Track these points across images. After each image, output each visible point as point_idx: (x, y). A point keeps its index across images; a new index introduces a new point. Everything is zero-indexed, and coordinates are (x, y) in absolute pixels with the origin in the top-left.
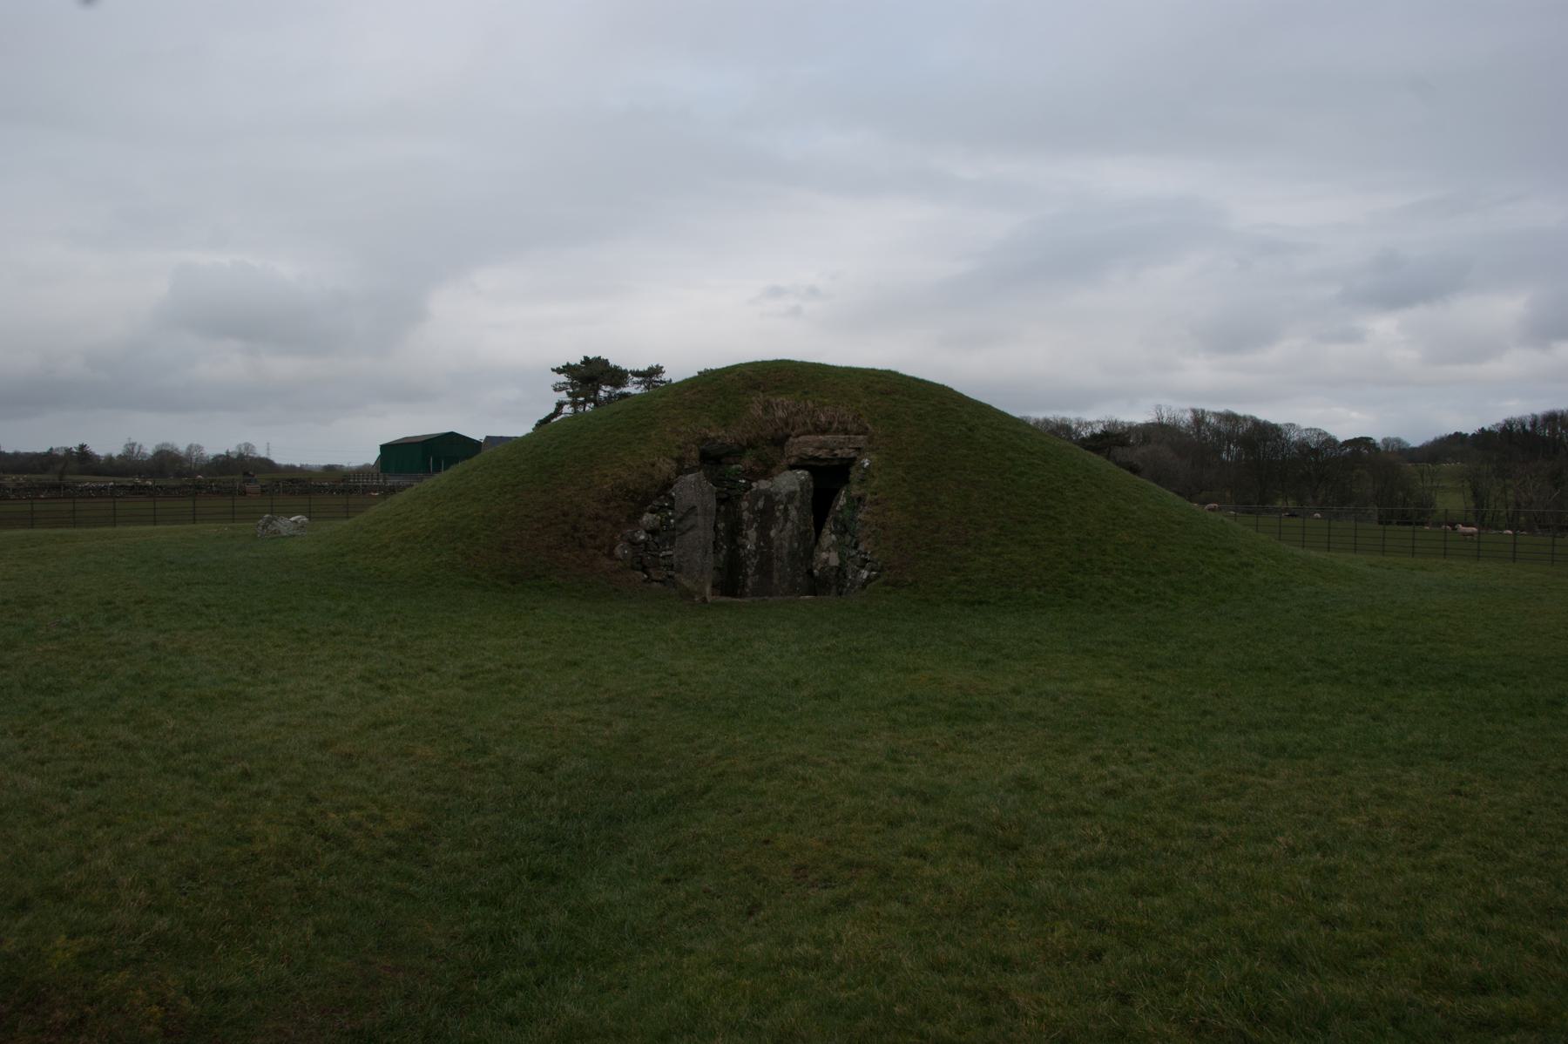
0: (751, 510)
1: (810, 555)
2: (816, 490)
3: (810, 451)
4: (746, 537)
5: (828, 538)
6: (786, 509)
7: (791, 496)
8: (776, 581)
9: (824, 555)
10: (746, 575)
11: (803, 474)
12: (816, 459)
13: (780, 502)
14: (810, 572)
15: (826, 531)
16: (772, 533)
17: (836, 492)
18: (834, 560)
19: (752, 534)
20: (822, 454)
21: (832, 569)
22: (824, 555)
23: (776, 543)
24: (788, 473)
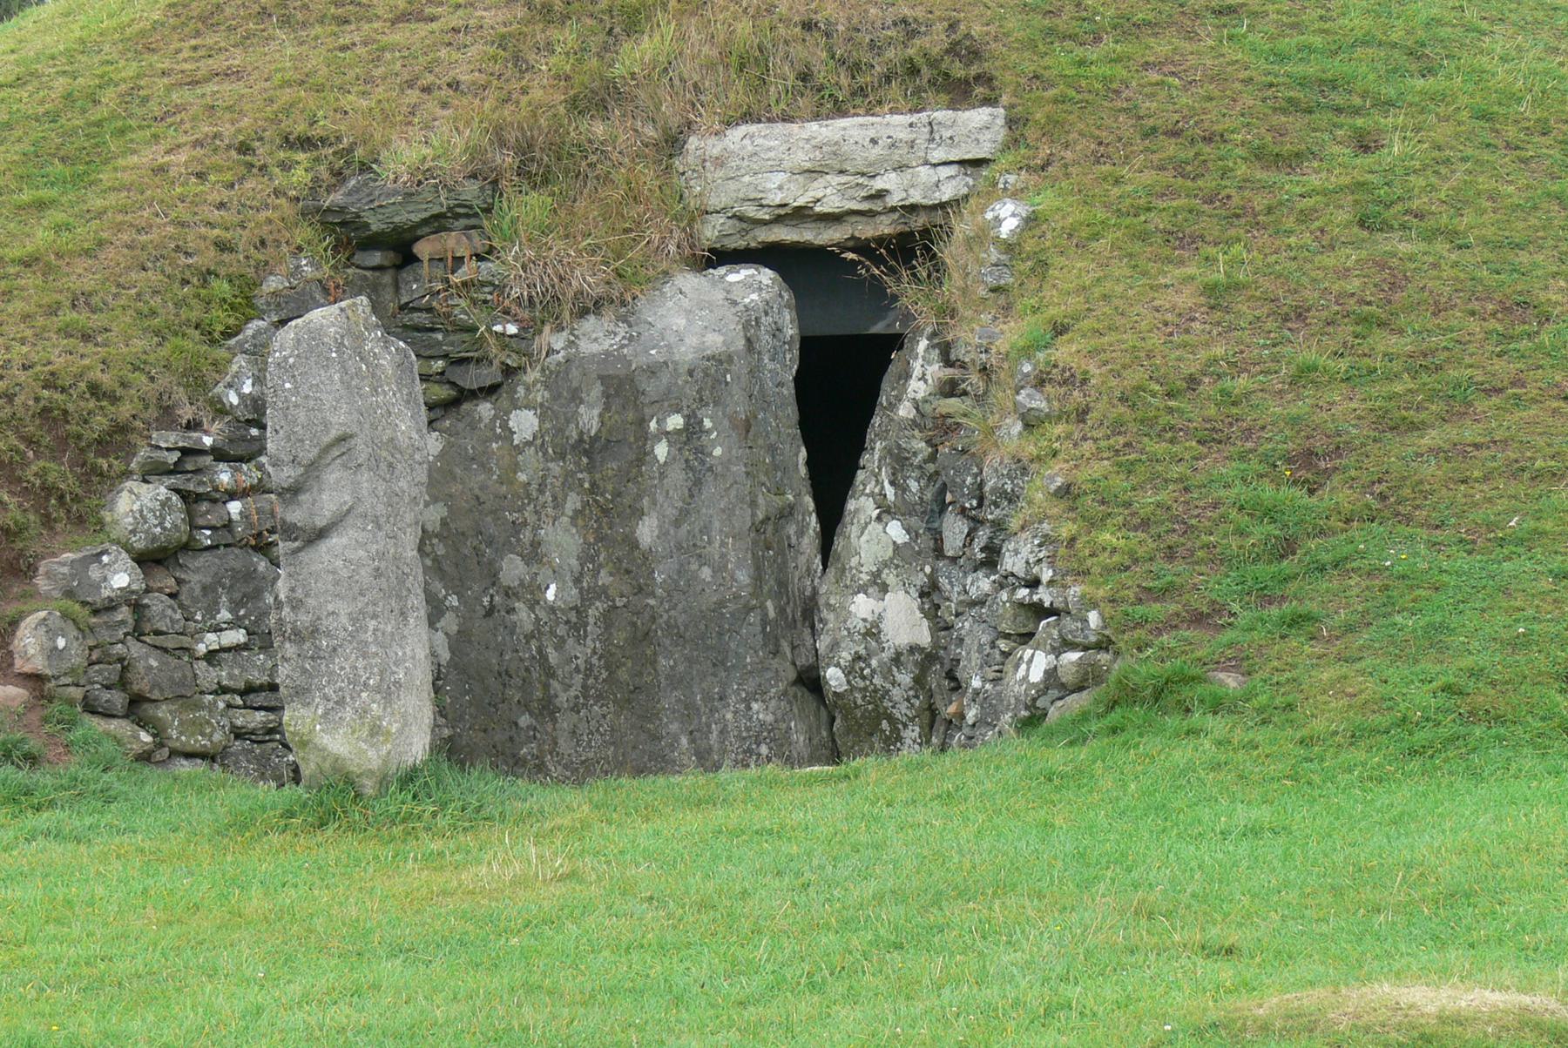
3: (780, 189)
5: (873, 534)
9: (863, 606)
11: (754, 285)
12: (801, 215)
20: (829, 195)
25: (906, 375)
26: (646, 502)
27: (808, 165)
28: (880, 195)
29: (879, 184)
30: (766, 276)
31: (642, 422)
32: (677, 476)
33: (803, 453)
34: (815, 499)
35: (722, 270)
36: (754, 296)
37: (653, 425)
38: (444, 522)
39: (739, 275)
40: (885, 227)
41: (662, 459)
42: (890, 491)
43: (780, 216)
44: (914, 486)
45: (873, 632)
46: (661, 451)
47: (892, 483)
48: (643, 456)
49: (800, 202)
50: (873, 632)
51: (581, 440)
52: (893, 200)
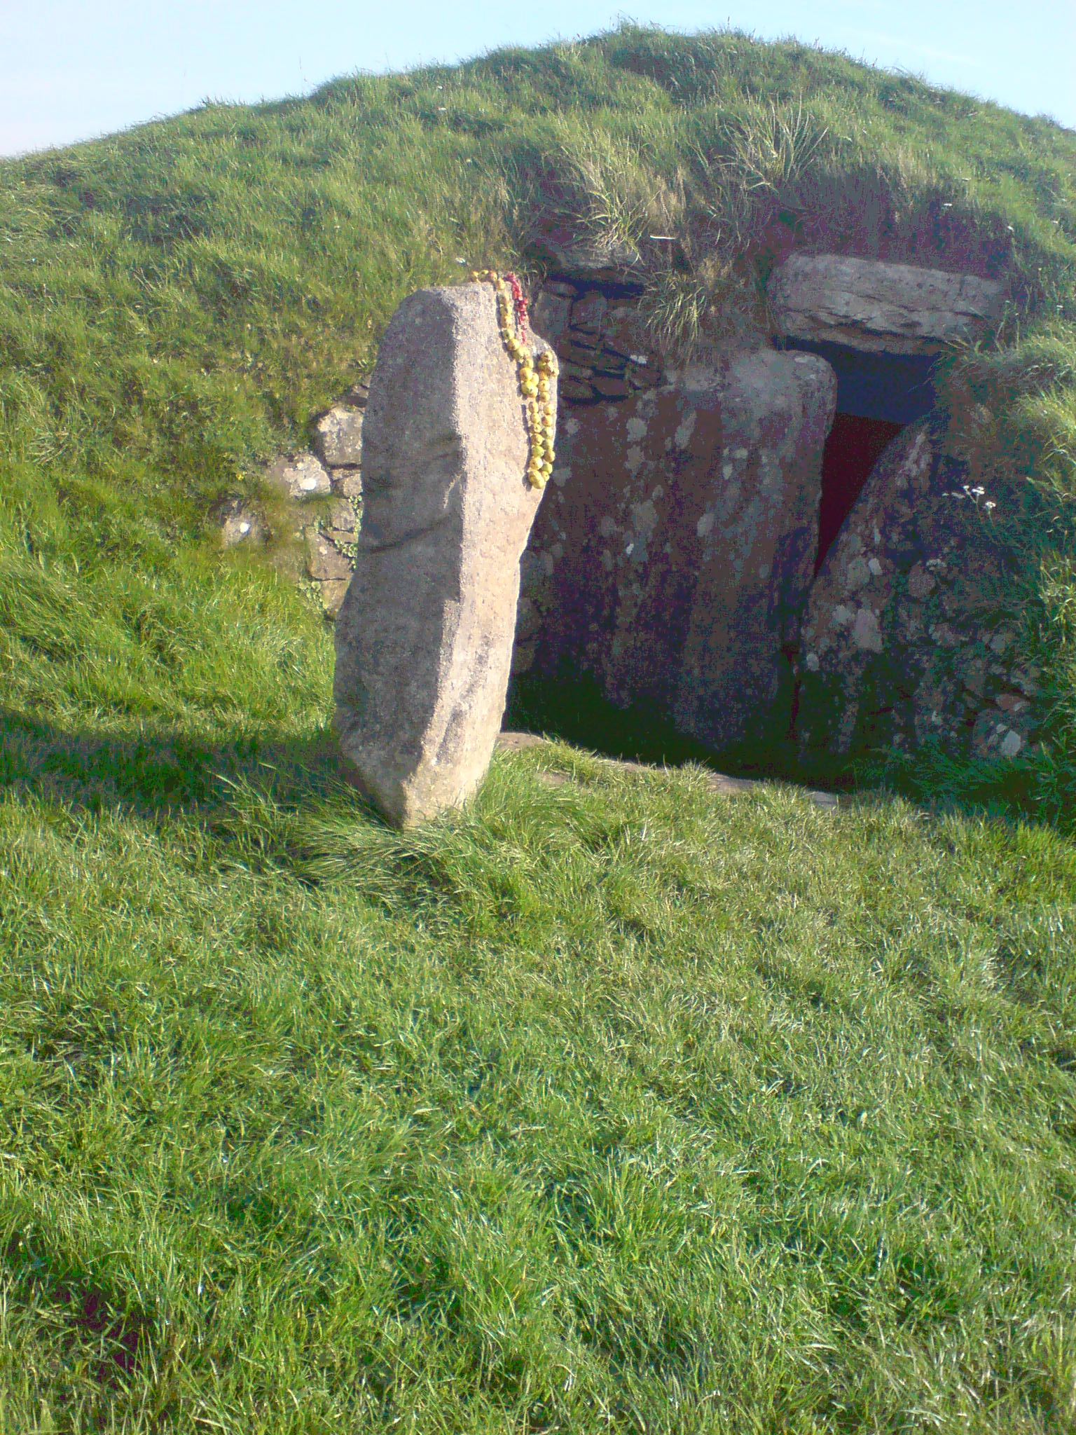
0: (650, 445)
1: (790, 607)
3: (845, 304)
4: (625, 519)
5: (859, 565)
6: (753, 461)
7: (774, 426)
9: (842, 614)
10: (610, 625)
11: (814, 369)
13: (740, 438)
14: (792, 651)
17: (893, 431)
18: (867, 631)
19: (645, 514)
20: (877, 317)
21: (857, 657)
22: (842, 614)
24: (769, 355)
25: (902, 457)
26: (709, 504)
27: (870, 292)
28: (914, 325)
29: (915, 317)
30: (822, 364)
31: (719, 449)
32: (734, 491)
33: (820, 495)
35: (793, 352)
36: (813, 376)
37: (726, 452)
39: (804, 359)
41: (726, 478)
42: (878, 538)
43: (841, 324)
44: (895, 537)
45: (844, 634)
46: (727, 471)
47: (882, 532)
48: (714, 471)
49: (859, 317)
50: (844, 634)
51: (673, 450)
52: (924, 331)
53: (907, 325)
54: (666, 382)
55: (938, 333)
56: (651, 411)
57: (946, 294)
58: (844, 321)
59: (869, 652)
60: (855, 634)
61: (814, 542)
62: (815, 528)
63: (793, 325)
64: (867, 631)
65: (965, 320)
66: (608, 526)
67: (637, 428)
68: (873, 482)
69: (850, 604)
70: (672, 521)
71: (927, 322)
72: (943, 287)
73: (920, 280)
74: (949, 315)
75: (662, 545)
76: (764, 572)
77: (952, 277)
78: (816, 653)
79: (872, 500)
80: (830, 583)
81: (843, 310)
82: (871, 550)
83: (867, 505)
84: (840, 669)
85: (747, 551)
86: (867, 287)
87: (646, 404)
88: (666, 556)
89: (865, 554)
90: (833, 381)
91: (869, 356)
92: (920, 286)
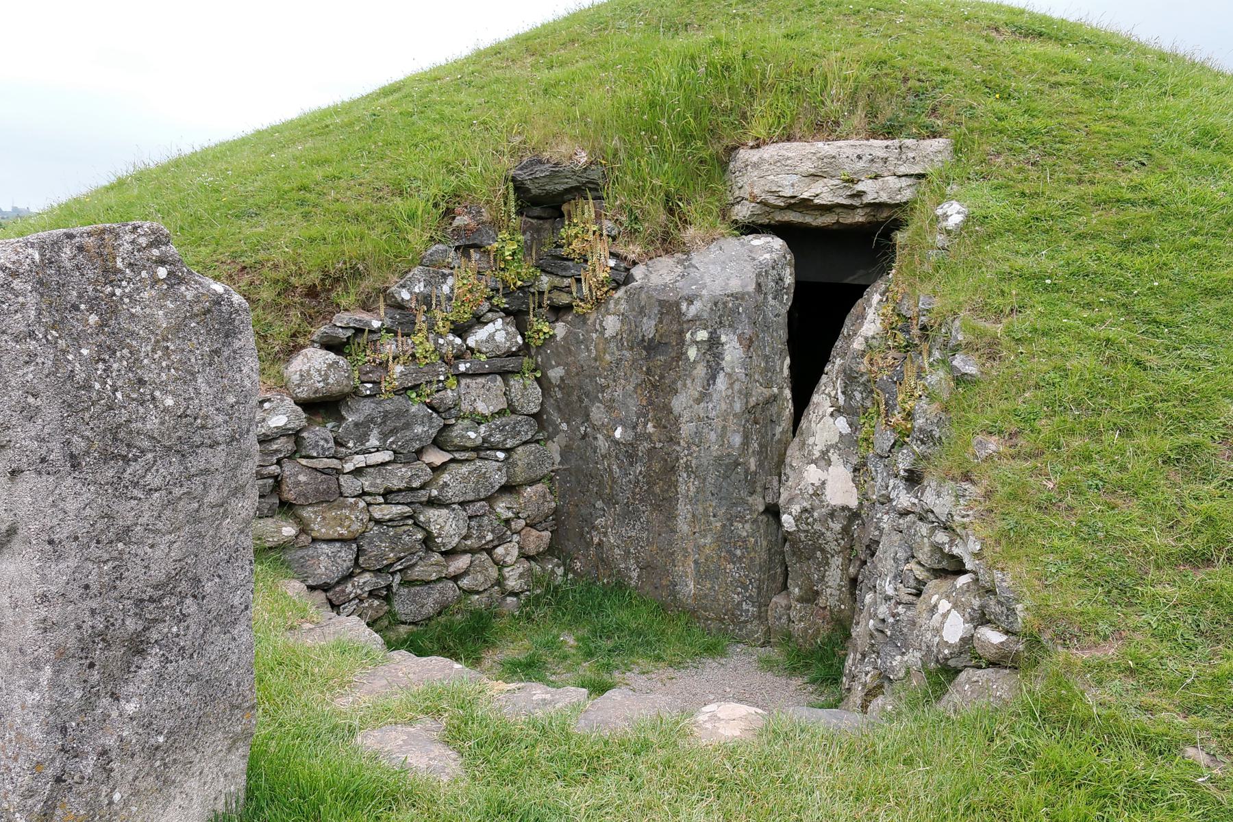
2: (801, 288)
3: (790, 186)
5: (825, 424)
6: (713, 343)
8: (683, 527)
9: (812, 474)
11: (771, 247)
12: (804, 205)
14: (773, 512)
15: (822, 400)
16: (679, 403)
17: (857, 292)
20: (823, 192)
23: (687, 429)
25: (862, 317)
26: (679, 384)
27: (813, 171)
28: (860, 194)
29: (860, 187)
30: (778, 243)
31: (681, 333)
32: (701, 371)
33: (788, 361)
34: (793, 391)
35: (751, 237)
36: (767, 256)
37: (688, 335)
38: (562, 379)
39: (758, 241)
40: (859, 217)
41: (692, 359)
42: (841, 398)
43: (791, 204)
44: (858, 396)
45: (818, 491)
46: (692, 353)
47: (843, 393)
48: (681, 355)
49: (806, 195)
50: (818, 491)
51: (643, 340)
52: (868, 199)
53: (852, 196)
54: (634, 280)
55: (884, 198)
56: (623, 306)
57: (885, 160)
58: (792, 201)
59: (844, 508)
60: (828, 491)
61: (789, 407)
62: (788, 393)
63: (742, 212)
64: (840, 488)
65: (905, 182)
66: (598, 413)
67: (612, 324)
68: (838, 344)
69: (823, 463)
70: (650, 403)
71: (872, 191)
72: (882, 154)
73: (859, 151)
74: (891, 180)
75: (645, 425)
76: (737, 440)
77: (889, 143)
78: (790, 514)
79: (838, 361)
80: (803, 444)
81: (788, 192)
82: (838, 411)
83: (835, 366)
84: (817, 527)
85: (717, 423)
86: (808, 167)
87: (617, 302)
88: (650, 435)
89: (832, 415)
90: (788, 257)
91: (818, 230)
92: (859, 157)
